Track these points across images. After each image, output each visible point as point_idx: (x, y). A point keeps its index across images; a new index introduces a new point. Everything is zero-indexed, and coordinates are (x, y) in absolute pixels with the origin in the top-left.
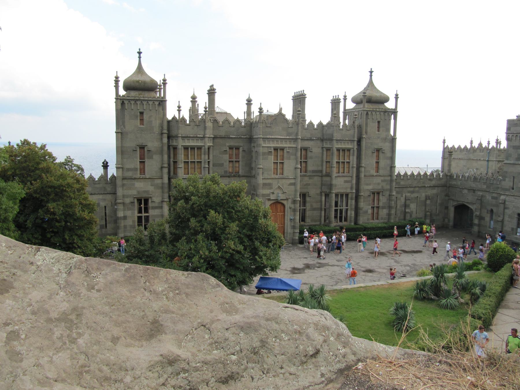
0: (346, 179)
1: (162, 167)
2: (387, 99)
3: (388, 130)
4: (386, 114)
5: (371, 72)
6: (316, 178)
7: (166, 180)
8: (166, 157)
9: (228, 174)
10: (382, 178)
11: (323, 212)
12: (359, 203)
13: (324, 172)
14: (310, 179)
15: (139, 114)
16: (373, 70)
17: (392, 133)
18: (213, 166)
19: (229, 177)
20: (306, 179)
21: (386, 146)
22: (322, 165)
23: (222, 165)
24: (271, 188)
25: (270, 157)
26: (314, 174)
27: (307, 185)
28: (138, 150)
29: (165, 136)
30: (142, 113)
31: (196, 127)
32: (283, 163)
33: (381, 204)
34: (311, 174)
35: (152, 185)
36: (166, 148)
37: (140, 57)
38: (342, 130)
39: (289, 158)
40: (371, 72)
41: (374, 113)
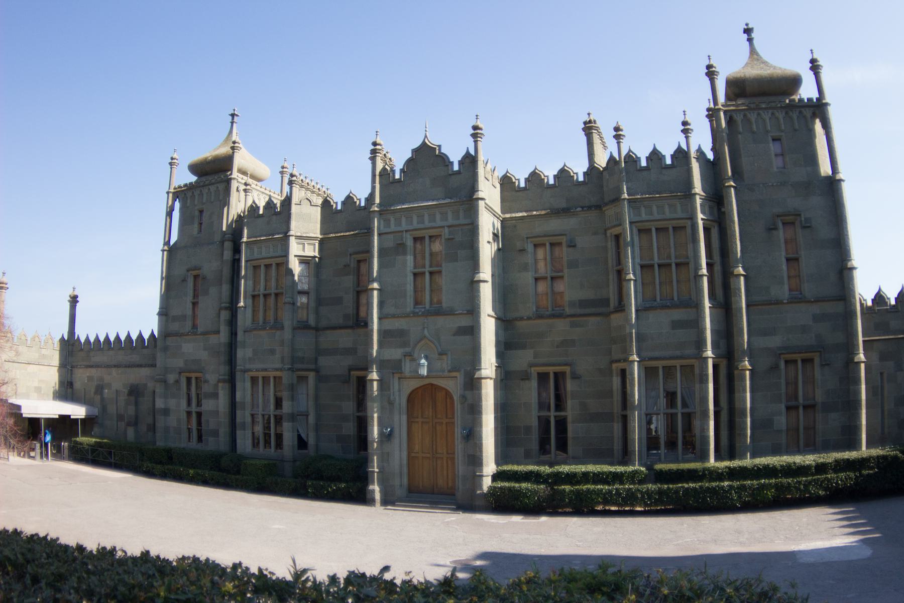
0: (678, 314)
1: (221, 309)
2: (794, 82)
3: (812, 159)
4: (795, 115)
5: (748, 31)
6: (592, 320)
7: (223, 336)
8: (226, 288)
9: (351, 323)
10: (816, 309)
11: (617, 427)
12: (737, 395)
13: (613, 302)
14: (573, 325)
15: (197, 213)
16: (750, 26)
17: (825, 169)
18: (320, 302)
19: (351, 327)
20: (561, 325)
21: (815, 205)
22: (608, 286)
23: (339, 301)
24: (405, 344)
25: (400, 258)
26: (588, 311)
27: (565, 343)
28: (191, 281)
29: (228, 245)
30: (201, 212)
31: (274, 217)
32: (440, 272)
33: (819, 397)
34: (579, 311)
35: (205, 349)
36: (227, 272)
37: (232, 123)
38: (647, 169)
39: (453, 258)
40: (748, 31)
41: (753, 117)
